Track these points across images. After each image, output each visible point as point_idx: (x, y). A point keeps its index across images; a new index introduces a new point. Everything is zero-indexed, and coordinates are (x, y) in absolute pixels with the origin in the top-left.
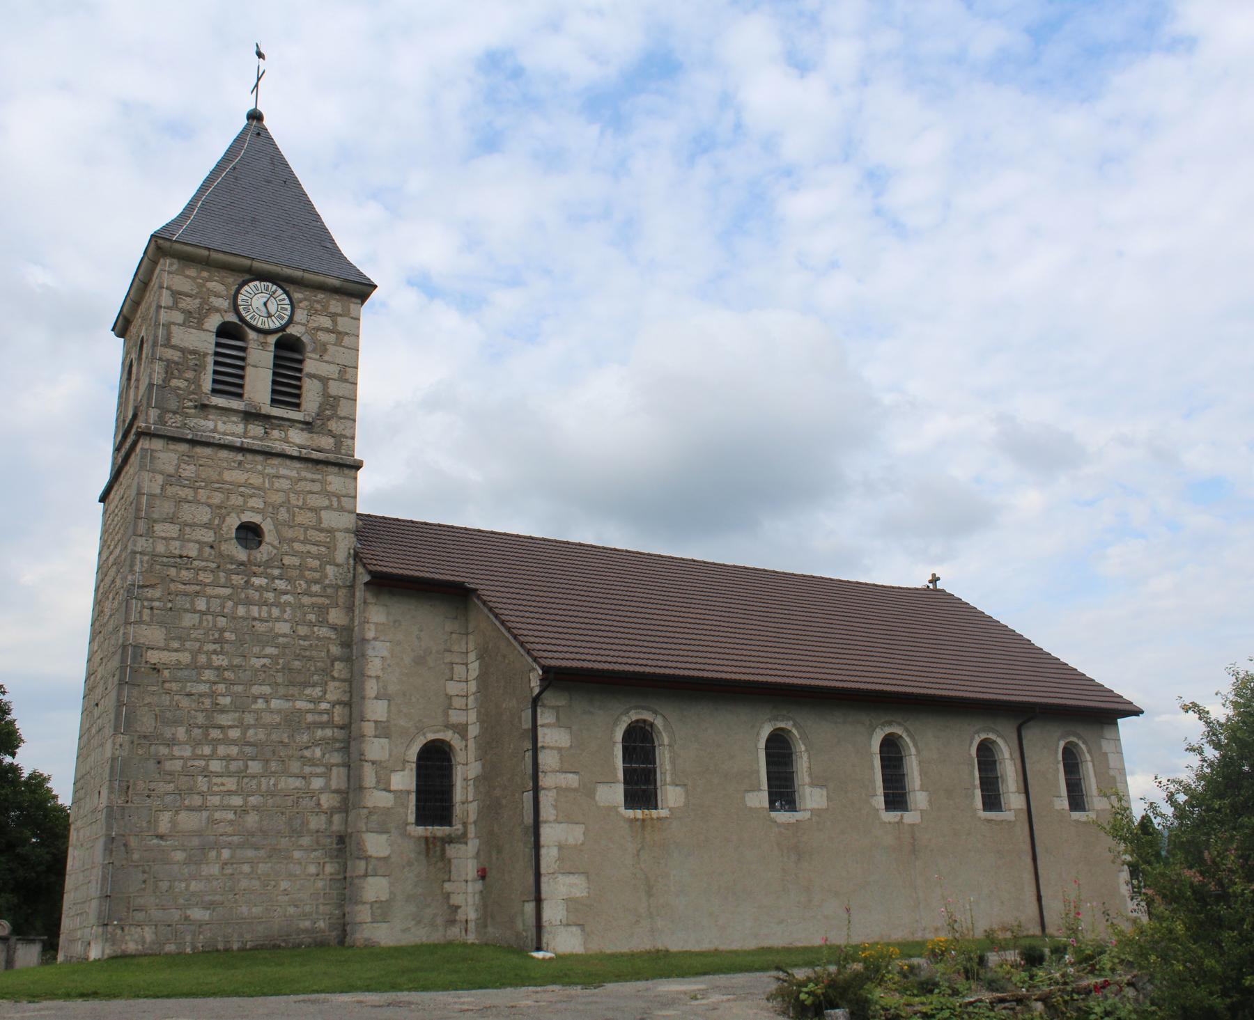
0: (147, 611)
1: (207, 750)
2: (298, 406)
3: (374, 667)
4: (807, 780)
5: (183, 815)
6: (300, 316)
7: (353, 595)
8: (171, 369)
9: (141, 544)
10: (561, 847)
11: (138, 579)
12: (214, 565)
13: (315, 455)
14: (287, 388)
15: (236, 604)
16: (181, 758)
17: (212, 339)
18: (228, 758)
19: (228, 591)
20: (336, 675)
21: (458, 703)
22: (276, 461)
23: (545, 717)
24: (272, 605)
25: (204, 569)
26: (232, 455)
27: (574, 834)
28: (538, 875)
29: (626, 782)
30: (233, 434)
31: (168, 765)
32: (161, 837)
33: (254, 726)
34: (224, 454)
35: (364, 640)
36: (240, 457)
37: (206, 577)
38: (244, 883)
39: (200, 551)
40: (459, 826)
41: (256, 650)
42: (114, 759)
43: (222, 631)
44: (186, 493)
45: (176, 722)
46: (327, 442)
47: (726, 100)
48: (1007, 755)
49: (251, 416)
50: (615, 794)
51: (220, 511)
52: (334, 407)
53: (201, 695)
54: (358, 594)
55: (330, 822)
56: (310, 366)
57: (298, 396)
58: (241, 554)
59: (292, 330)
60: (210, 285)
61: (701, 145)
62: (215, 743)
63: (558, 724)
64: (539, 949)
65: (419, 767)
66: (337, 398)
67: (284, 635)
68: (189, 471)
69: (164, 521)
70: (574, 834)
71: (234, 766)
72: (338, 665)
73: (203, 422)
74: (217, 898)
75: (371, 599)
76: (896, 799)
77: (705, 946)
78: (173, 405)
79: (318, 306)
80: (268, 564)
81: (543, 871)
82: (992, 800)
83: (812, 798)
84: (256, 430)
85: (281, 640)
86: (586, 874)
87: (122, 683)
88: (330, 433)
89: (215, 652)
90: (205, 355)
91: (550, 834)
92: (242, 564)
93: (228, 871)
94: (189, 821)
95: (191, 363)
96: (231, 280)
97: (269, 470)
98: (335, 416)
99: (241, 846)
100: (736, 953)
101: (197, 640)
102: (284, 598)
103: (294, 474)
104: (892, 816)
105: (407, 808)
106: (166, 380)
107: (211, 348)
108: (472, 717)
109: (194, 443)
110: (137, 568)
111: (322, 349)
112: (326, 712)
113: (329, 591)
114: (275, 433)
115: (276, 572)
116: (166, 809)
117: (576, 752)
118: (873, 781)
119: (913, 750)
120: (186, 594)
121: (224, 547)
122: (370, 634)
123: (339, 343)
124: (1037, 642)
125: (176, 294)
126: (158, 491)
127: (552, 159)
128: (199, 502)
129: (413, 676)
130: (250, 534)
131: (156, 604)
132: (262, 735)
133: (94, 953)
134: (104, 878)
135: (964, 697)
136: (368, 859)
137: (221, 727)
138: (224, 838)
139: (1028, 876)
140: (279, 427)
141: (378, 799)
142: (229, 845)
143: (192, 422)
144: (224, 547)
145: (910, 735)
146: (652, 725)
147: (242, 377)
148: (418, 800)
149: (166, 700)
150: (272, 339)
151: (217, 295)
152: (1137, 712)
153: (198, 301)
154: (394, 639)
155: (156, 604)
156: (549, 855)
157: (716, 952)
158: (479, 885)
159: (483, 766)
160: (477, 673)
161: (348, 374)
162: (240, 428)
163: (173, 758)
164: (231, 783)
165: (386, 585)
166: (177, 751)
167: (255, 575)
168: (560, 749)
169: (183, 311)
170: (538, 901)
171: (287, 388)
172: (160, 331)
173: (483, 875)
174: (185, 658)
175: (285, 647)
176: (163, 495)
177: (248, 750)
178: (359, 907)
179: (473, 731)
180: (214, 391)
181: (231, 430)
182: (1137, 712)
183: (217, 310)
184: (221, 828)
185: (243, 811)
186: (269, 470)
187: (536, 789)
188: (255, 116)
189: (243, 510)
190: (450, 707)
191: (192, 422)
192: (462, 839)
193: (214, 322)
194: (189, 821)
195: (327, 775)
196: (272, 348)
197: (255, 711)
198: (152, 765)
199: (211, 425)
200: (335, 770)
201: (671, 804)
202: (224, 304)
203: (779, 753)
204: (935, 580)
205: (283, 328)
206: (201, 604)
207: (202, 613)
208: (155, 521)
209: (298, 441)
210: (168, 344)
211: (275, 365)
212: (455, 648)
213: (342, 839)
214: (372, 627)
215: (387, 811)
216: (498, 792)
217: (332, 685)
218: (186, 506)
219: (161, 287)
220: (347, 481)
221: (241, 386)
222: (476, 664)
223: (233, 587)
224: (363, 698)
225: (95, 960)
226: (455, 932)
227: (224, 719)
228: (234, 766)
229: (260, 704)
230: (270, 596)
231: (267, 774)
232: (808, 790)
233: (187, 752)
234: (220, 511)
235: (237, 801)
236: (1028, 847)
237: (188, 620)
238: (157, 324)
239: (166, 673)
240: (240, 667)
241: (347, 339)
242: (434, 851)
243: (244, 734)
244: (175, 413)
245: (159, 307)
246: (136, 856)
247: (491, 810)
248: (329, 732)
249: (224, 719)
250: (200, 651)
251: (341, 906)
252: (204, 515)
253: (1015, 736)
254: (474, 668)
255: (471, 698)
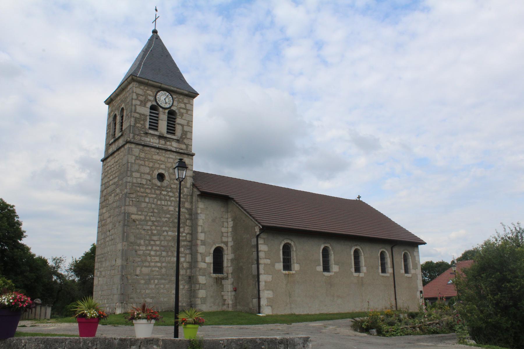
0: (131, 202)
1: (150, 248)
2: (174, 134)
3: (200, 222)
4: (333, 262)
5: (143, 269)
6: (175, 103)
7: (192, 198)
8: (137, 120)
9: (129, 179)
10: (265, 282)
11: (129, 191)
12: (150, 187)
13: (181, 151)
14: (171, 129)
15: (158, 200)
16: (142, 250)
17: (149, 110)
18: (156, 251)
19: (154, 196)
20: (187, 224)
21: (225, 235)
22: (169, 153)
23: (261, 241)
24: (168, 201)
25: (148, 188)
26: (155, 150)
27: (269, 278)
28: (259, 291)
29: (283, 262)
30: (155, 143)
31: (139, 252)
32: (137, 275)
33: (164, 241)
34: (153, 150)
35: (197, 213)
36: (158, 151)
37: (148, 191)
38: (162, 291)
39: (146, 182)
40: (226, 274)
41: (164, 215)
42: (123, 250)
43: (153, 209)
44: (142, 162)
45: (141, 239)
46: (184, 147)
47: (269, 13)
48: (388, 256)
49: (161, 137)
50: (280, 266)
51: (152, 169)
52: (186, 135)
53: (148, 230)
54: (194, 198)
55: (186, 272)
56: (178, 120)
57: (174, 131)
58: (159, 184)
59: (173, 108)
60: (148, 92)
61: (258, 28)
62: (152, 246)
63: (265, 243)
64: (259, 313)
65: (214, 255)
66: (186, 132)
67: (172, 211)
68: (142, 155)
69: (135, 172)
70: (269, 278)
71: (158, 253)
72: (188, 221)
73: (146, 139)
74: (154, 295)
75: (199, 200)
76: (358, 269)
77: (305, 313)
78: (137, 132)
79: (181, 100)
80: (166, 187)
81: (260, 289)
82: (384, 270)
83: (335, 268)
84: (162, 142)
85: (171, 212)
86: (272, 290)
87: (124, 225)
88: (185, 144)
89: (151, 216)
90: (147, 116)
91: (262, 278)
92: (159, 187)
93: (157, 287)
94: (145, 270)
95: (142, 118)
96: (154, 90)
97: (167, 156)
98: (186, 137)
99: (161, 279)
100: (313, 315)
101: (146, 212)
102: (172, 198)
103: (174, 157)
104: (356, 274)
105: (210, 268)
106: (135, 124)
107: (148, 114)
108: (230, 239)
109: (144, 146)
110: (128, 187)
111: (182, 115)
112: (185, 236)
113: (185, 197)
114: (168, 143)
115: (169, 190)
116: (138, 267)
117: (269, 251)
118: (351, 263)
119: (363, 254)
120: (142, 196)
121: (154, 181)
122: (199, 212)
123: (187, 113)
124: (393, 219)
125: (137, 95)
126: (133, 162)
127: (203, 28)
128: (146, 166)
129: (212, 226)
130: (161, 177)
131: (134, 199)
132: (166, 244)
133: (118, 311)
134: (121, 288)
135: (361, 234)
136: (199, 284)
137: (154, 240)
138: (155, 276)
139: (393, 293)
140: (169, 141)
141: (202, 265)
142: (157, 279)
143: (143, 138)
144: (154, 181)
145: (362, 249)
146: (290, 244)
147: (157, 124)
148: (214, 266)
149: (137, 231)
150: (167, 111)
151: (150, 95)
152: (425, 243)
153: (144, 97)
154: (206, 213)
155: (134, 199)
156: (262, 284)
157: (308, 315)
158: (233, 293)
159: (235, 256)
160: (232, 225)
161: (190, 123)
162: (157, 141)
163: (140, 250)
164: (157, 259)
165: (205, 195)
166: (141, 248)
167: (163, 190)
168: (265, 251)
169: (140, 101)
170: (259, 298)
171: (171, 129)
172: (133, 108)
173: (235, 290)
174: (143, 217)
175: (172, 215)
176: (135, 163)
177: (162, 248)
178: (197, 299)
179: (230, 244)
180: (150, 128)
181: (155, 142)
182: (425, 243)
183: (150, 101)
184: (155, 273)
185: (161, 268)
186: (167, 156)
187: (258, 264)
188: (155, 32)
189: (159, 168)
190: (223, 236)
191: (143, 138)
192: (227, 278)
193: (149, 105)
194: (145, 270)
195: (185, 257)
196: (167, 114)
197: (164, 236)
198: (134, 252)
199: (148, 140)
200: (187, 256)
201: (296, 269)
202: (152, 98)
203: (326, 253)
204: (359, 197)
205: (170, 108)
206: (147, 200)
207: (148, 203)
208: (133, 172)
209: (175, 146)
210: (135, 112)
211: (168, 120)
212: (224, 217)
213: (190, 277)
214: (200, 209)
215: (205, 269)
216: (241, 264)
217: (186, 228)
218: (142, 167)
219: (133, 92)
220: (190, 160)
221: (157, 127)
222: (232, 222)
223: (156, 194)
224: (197, 232)
225: (120, 314)
226: (225, 308)
227: (155, 238)
228: (158, 253)
229: (165, 233)
230: (167, 197)
231: (168, 256)
232: (333, 266)
233: (144, 248)
234: (152, 169)
235: (159, 264)
236: (393, 283)
237: (143, 205)
238: (132, 105)
239: (137, 222)
240: (159, 221)
241: (189, 111)
242: (219, 282)
243: (161, 243)
244: (138, 135)
245: (133, 99)
246: (130, 281)
247: (238, 270)
248: (185, 243)
249: (155, 238)
250: (147, 215)
251: (190, 299)
252: (147, 170)
253: (390, 250)
254: (231, 224)
255: (229, 234)
